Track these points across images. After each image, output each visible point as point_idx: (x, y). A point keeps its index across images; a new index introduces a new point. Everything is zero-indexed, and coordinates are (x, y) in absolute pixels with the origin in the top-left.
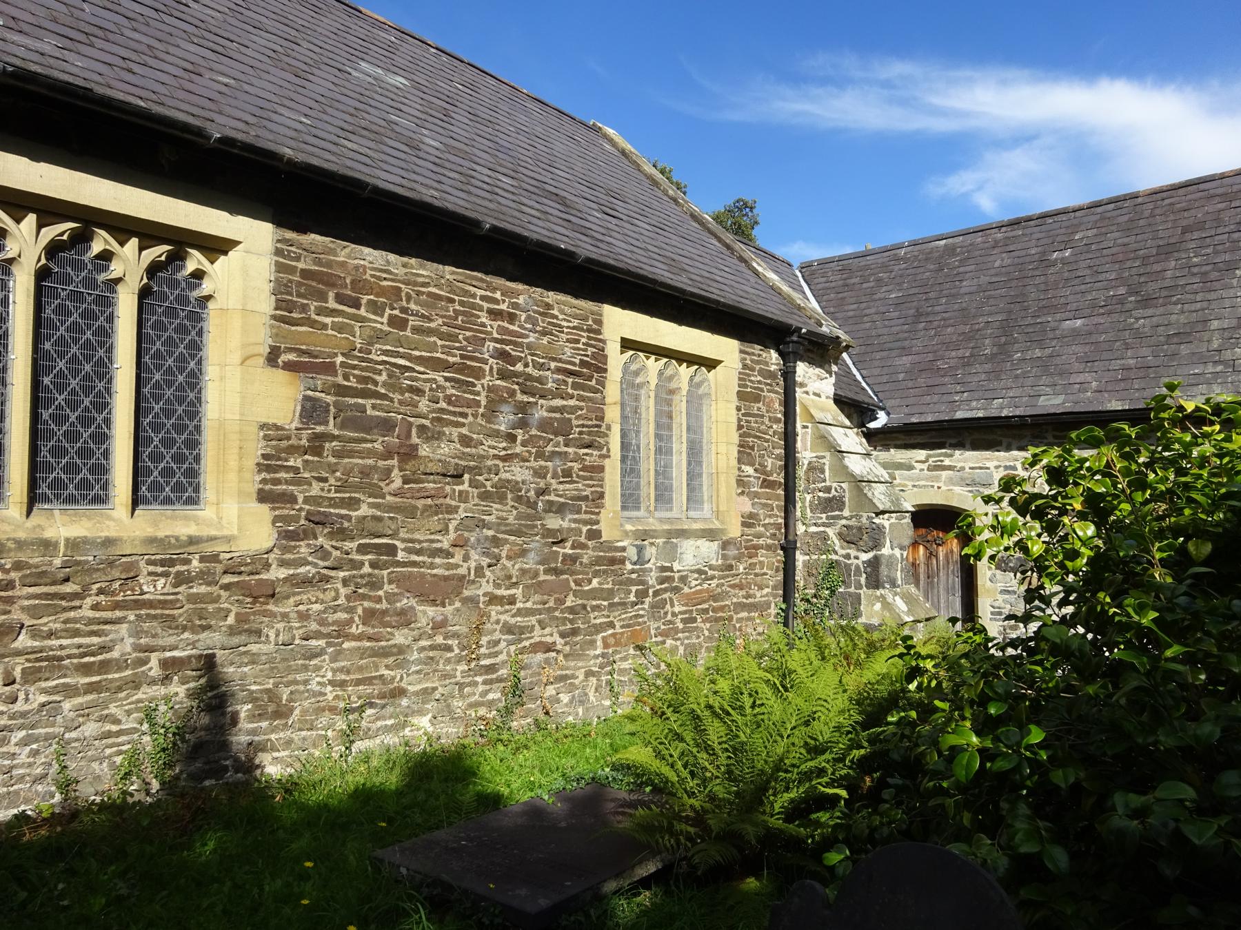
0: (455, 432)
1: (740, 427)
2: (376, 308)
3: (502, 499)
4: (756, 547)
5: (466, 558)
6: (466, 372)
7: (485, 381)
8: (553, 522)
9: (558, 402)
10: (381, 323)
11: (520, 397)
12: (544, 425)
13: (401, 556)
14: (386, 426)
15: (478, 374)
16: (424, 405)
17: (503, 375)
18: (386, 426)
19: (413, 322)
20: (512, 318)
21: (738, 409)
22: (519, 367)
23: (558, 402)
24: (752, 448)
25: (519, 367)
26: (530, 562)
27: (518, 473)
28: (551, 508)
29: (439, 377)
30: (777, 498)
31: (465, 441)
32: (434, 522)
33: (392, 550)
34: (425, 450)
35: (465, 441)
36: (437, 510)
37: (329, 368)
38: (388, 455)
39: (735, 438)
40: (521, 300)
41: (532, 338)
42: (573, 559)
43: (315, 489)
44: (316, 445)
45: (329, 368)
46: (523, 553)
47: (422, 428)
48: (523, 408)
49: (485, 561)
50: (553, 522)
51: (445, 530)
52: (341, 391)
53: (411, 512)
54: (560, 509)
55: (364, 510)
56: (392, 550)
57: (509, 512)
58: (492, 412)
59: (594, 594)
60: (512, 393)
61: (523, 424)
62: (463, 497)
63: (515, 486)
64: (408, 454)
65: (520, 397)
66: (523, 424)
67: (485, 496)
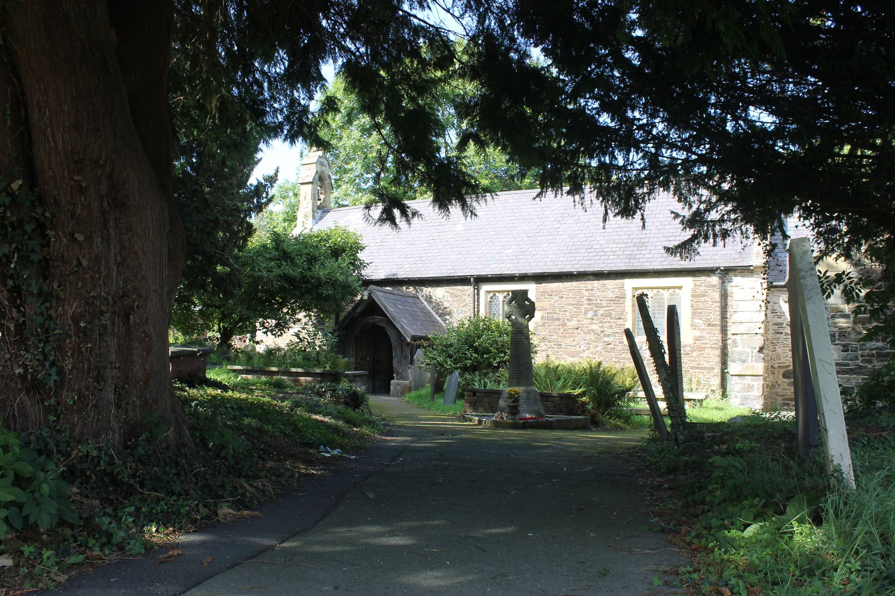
0: (576, 319)
1: (692, 306)
2: (556, 295)
3: (590, 333)
4: (704, 348)
5: (580, 347)
6: (578, 305)
7: (584, 306)
8: (606, 339)
9: (607, 309)
10: (557, 298)
11: (595, 309)
12: (602, 315)
13: (563, 346)
14: (558, 319)
15: (582, 305)
16: (568, 314)
17: (589, 304)
18: (558, 319)
19: (565, 296)
20: (592, 290)
21: (692, 301)
22: (594, 302)
23: (607, 309)
24: (701, 313)
25: (594, 302)
26: (599, 349)
27: (594, 327)
28: (605, 335)
29: (571, 307)
30: (717, 330)
31: (579, 321)
32: (571, 339)
33: (561, 345)
34: (568, 324)
35: (579, 321)
36: (572, 337)
37: (546, 309)
38: (559, 325)
39: (690, 311)
40: (595, 285)
41: (599, 294)
42: (614, 349)
43: (544, 333)
44: (544, 325)
45: (546, 309)
46: (597, 347)
47: (567, 319)
48: (596, 311)
49: (585, 348)
50: (606, 339)
51: (574, 341)
52: (548, 313)
53: (565, 337)
54: (609, 336)
55: (555, 337)
56: (561, 345)
57: (592, 337)
58: (586, 313)
59: (622, 358)
60: (592, 308)
61: (596, 315)
62: (579, 334)
63: (593, 331)
64: (565, 325)
65: (595, 309)
66: (596, 315)
67: (585, 333)
